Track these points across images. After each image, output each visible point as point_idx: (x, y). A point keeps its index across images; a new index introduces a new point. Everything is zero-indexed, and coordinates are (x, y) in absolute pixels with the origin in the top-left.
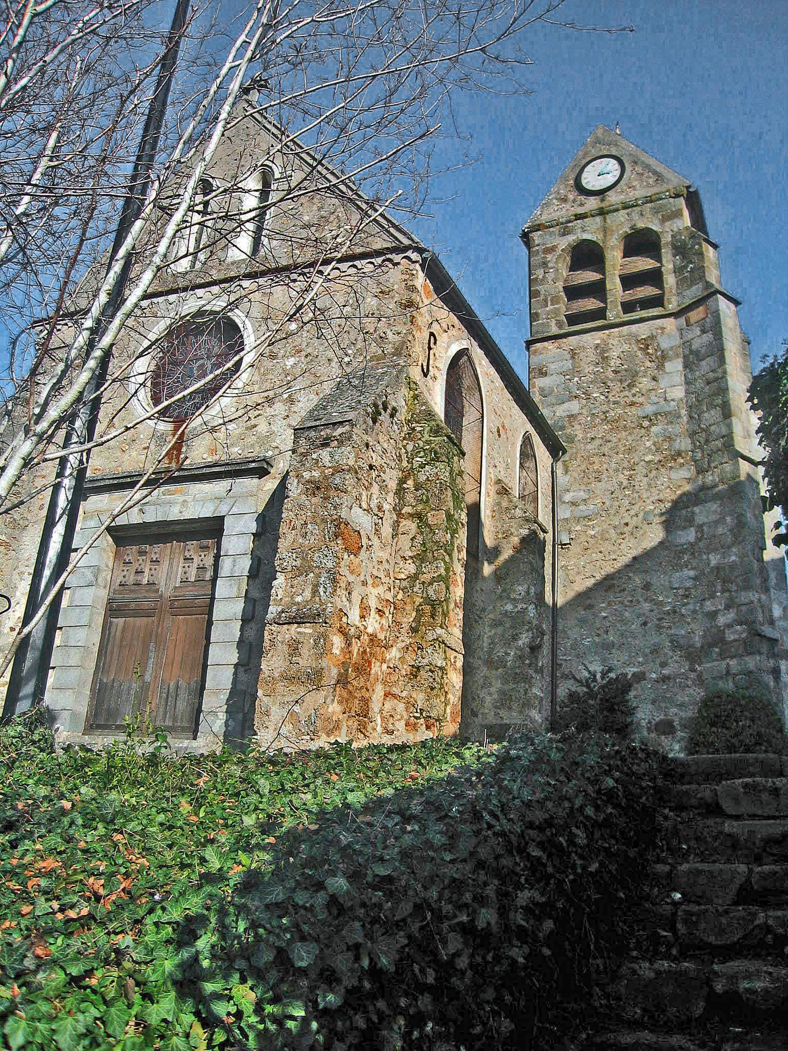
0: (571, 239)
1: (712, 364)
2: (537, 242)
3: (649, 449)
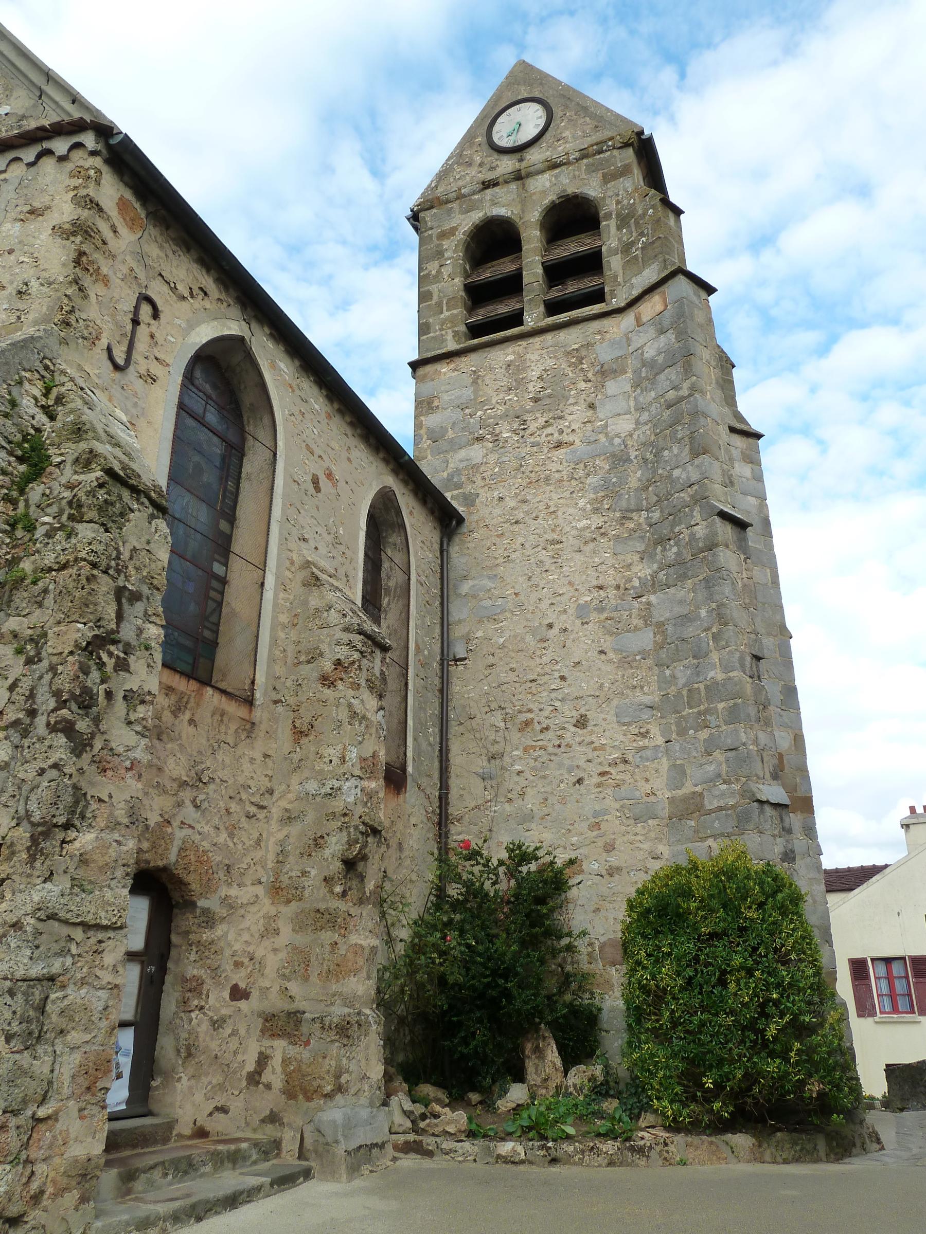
0: (477, 216)
1: (674, 378)
3: (583, 509)
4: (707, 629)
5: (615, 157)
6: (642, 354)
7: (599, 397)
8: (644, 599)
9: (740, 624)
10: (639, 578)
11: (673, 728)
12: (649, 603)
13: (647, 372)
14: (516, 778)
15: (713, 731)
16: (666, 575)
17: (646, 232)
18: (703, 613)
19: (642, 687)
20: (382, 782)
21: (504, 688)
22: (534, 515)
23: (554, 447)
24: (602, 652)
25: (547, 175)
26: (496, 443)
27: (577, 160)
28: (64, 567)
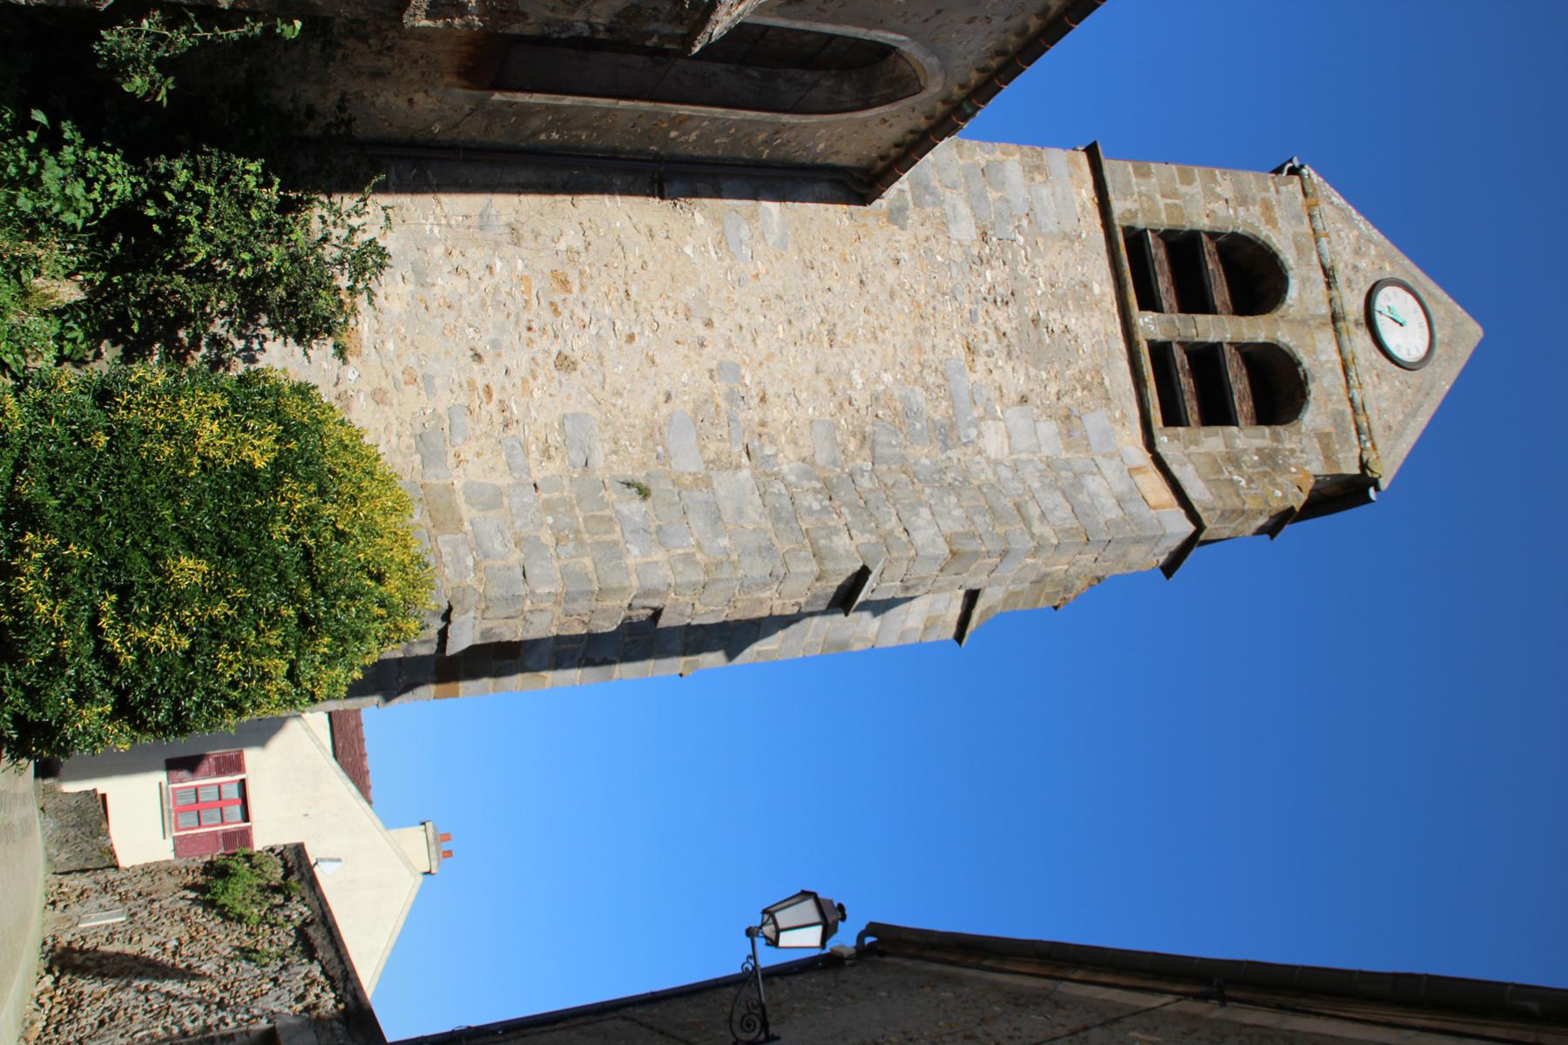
0: (1288, 256)
1: (1058, 514)
3: (878, 379)
4: (699, 545)
5: (1351, 450)
6: (1092, 473)
7: (1036, 411)
8: (745, 459)
9: (707, 593)
10: (775, 455)
11: (556, 495)
12: (738, 467)
13: (1066, 479)
14: (481, 265)
15: (552, 550)
16: (780, 494)
17: (1253, 486)
18: (724, 542)
19: (615, 452)
21: (618, 250)
22: (872, 309)
23: (968, 343)
24: (668, 397)
25: (1336, 357)
26: (978, 261)
27: (1351, 400)
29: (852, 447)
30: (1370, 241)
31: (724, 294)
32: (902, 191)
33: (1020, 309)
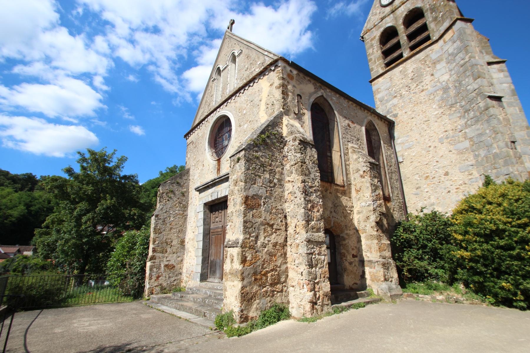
0: (382, 29)
2: (367, 38)
3: (435, 108)
6: (448, 52)
8: (463, 132)
10: (460, 125)
12: (465, 132)
14: (427, 194)
18: (488, 131)
19: (467, 160)
20: (383, 200)
21: (417, 168)
24: (450, 151)
25: (402, 7)
28: (296, 164)
29: (454, 109)
30: (372, 13)
31: (422, 145)
32: (390, 116)
33: (410, 83)
